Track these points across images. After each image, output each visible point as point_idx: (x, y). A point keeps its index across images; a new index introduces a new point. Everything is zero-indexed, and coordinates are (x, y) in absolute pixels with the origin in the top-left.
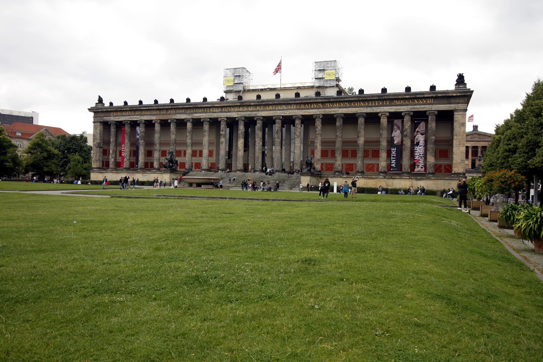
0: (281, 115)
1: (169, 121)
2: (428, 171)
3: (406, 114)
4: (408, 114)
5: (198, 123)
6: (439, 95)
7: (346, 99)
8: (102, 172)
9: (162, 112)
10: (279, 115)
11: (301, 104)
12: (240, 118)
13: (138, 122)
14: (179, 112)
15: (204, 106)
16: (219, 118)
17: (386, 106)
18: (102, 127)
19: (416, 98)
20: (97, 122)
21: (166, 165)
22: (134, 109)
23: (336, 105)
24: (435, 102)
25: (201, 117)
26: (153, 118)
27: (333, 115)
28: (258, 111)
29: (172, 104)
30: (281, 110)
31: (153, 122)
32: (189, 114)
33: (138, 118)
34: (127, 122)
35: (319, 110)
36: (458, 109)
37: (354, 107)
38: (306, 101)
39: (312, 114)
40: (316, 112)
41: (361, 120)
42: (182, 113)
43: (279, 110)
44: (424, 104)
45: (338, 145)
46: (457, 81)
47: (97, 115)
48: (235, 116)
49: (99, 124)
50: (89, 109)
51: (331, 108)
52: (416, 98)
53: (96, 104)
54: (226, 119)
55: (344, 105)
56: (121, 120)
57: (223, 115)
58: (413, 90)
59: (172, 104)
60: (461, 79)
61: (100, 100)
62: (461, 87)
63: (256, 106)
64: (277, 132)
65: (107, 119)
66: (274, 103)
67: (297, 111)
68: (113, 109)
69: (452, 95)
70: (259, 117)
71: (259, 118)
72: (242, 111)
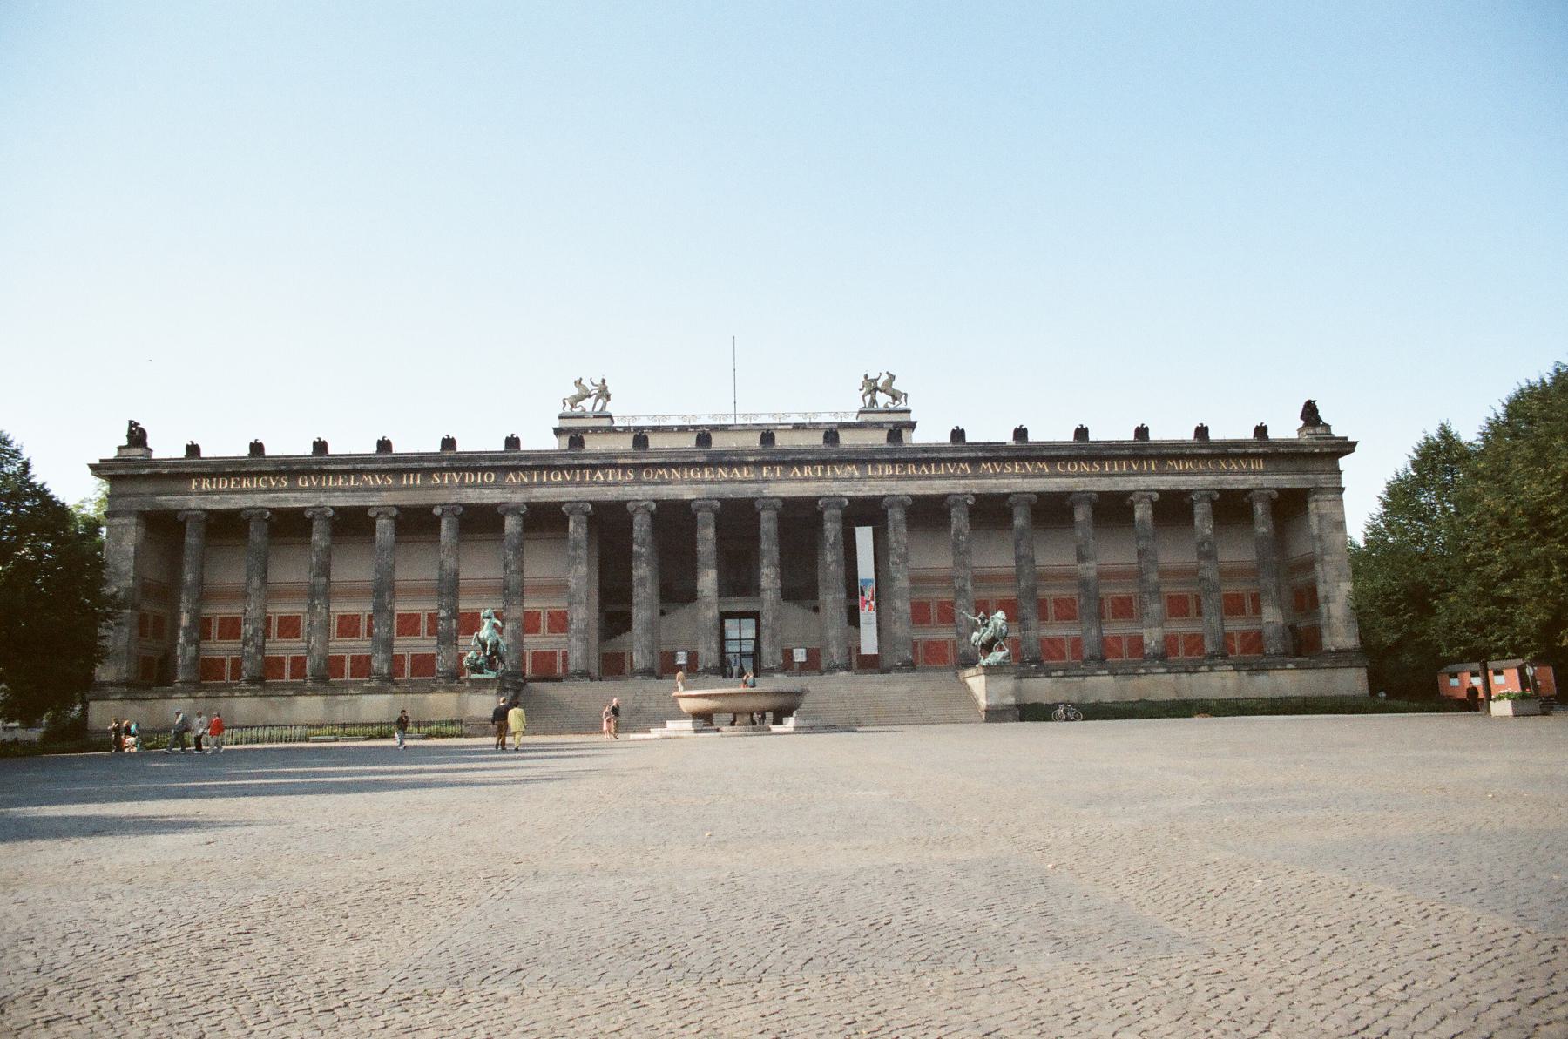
0: (844, 494)
1: (437, 511)
2: (1272, 650)
3: (1202, 496)
4: (1210, 496)
6: (1282, 450)
7: (1045, 453)
8: (145, 696)
9: (408, 478)
10: (837, 494)
12: (702, 502)
13: (309, 514)
14: (476, 481)
15: (576, 462)
17: (1150, 474)
18: (141, 530)
20: (129, 513)
21: (477, 659)
22: (295, 468)
23: (1013, 467)
24: (1271, 467)
25: (562, 500)
26: (373, 501)
27: (1007, 495)
28: (766, 481)
29: (447, 454)
30: (844, 480)
31: (372, 514)
32: (515, 488)
33: (307, 500)
34: (262, 514)
35: (962, 482)
36: (1325, 486)
37: (1067, 476)
38: (926, 455)
39: (941, 491)
40: (954, 488)
42: (484, 486)
43: (835, 479)
44: (1243, 473)
46: (1302, 417)
47: (125, 488)
48: (685, 498)
49: (134, 520)
50: (92, 467)
51: (996, 475)
52: (1227, 457)
53: (120, 448)
54: (654, 506)
55: (1034, 469)
56: (232, 506)
58: (1214, 436)
59: (447, 454)
60: (1310, 413)
61: (137, 436)
62: (1320, 432)
63: (758, 465)
64: (834, 546)
65: (171, 501)
66: (824, 457)
67: (894, 483)
68: (195, 466)
69: (1310, 449)
70: (774, 501)
72: (712, 482)
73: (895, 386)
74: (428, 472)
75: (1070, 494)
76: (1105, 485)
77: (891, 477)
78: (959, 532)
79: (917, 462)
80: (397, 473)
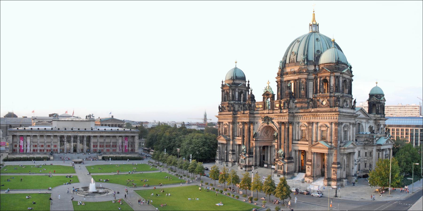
26: (37, 134)
32: (52, 134)
57: (65, 135)
63: (78, 132)
65: (15, 134)
71: (79, 136)
73: (93, 115)
74: (43, 132)
76: (113, 135)
79: (94, 132)
80: (40, 132)
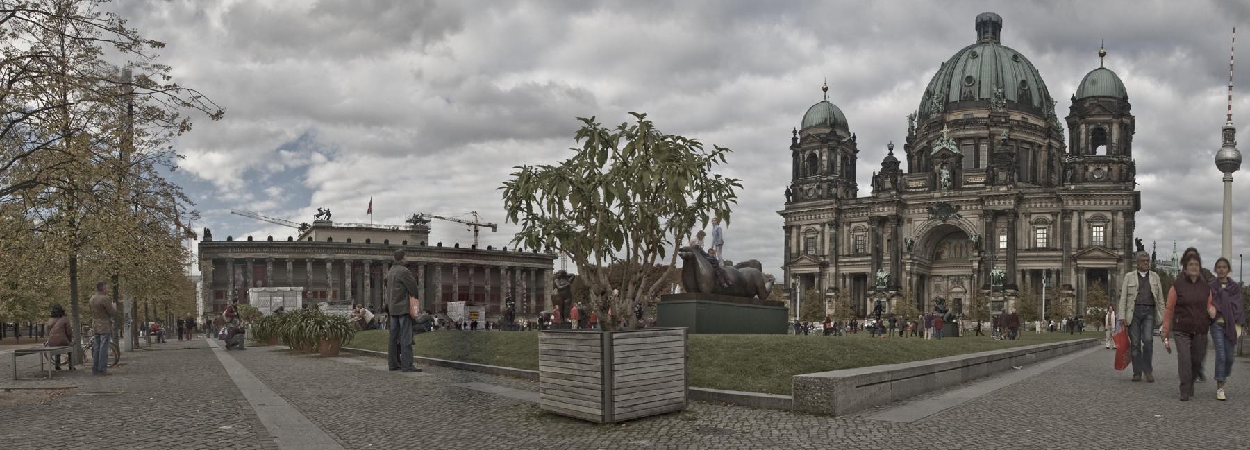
1: (307, 260)
5: (339, 264)
11: (442, 253)
13: (267, 260)
16: (363, 260)
19: (526, 258)
31: (287, 260)
32: (331, 254)
41: (487, 271)
42: (322, 253)
45: (472, 290)
52: (526, 258)
74: (304, 248)
75: (484, 265)
77: (438, 257)
78: (455, 275)
79: (445, 253)
80: (294, 248)
